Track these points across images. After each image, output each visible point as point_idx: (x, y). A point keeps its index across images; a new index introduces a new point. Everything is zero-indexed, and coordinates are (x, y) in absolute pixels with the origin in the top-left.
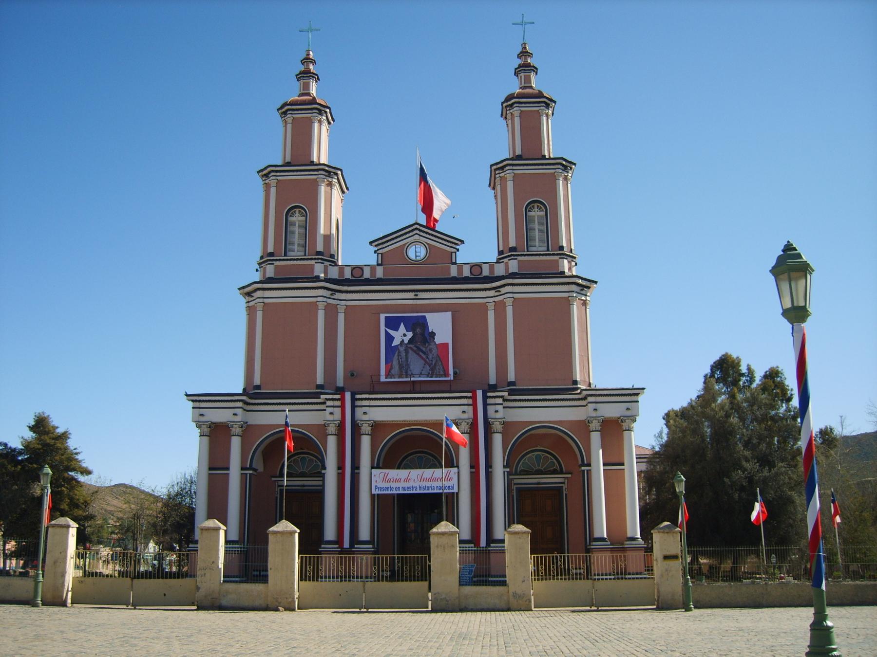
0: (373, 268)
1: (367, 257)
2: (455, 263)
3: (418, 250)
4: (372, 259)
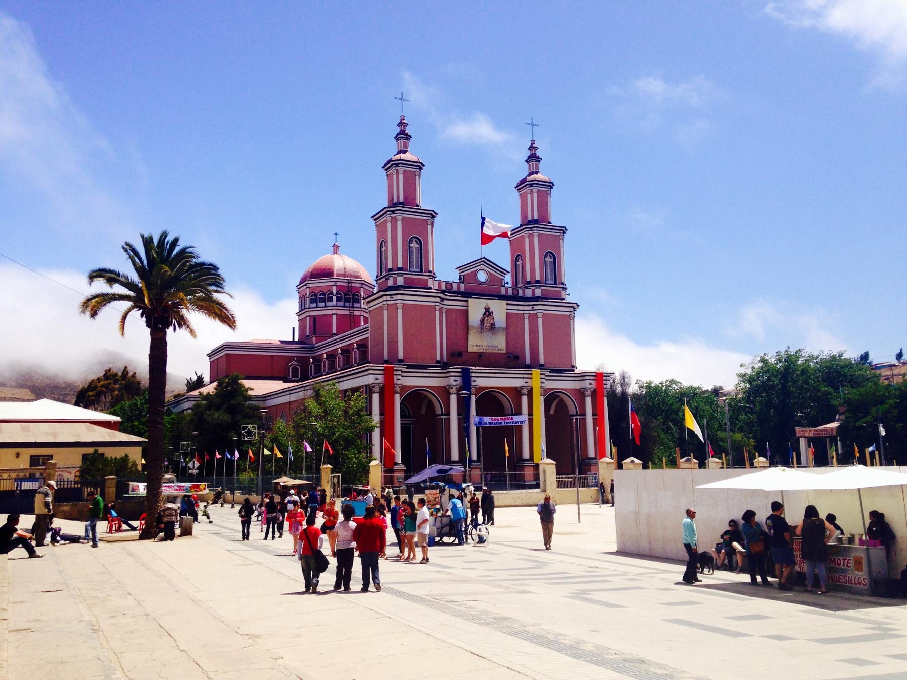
1: (454, 277)
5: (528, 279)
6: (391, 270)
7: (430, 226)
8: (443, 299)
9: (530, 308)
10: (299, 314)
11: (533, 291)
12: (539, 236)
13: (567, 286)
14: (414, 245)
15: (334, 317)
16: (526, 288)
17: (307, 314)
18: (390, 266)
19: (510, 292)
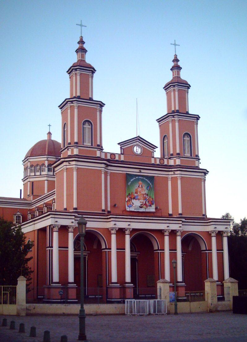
0: (119, 155)
1: (117, 150)
2: (153, 157)
3: (137, 149)
4: (119, 151)
5: (171, 152)
6: (70, 144)
7: (98, 113)
8: (107, 165)
10: (24, 180)
12: (179, 121)
13: (200, 158)
15: (46, 182)
16: (170, 158)
17: (28, 180)
18: (69, 141)
19: (158, 162)
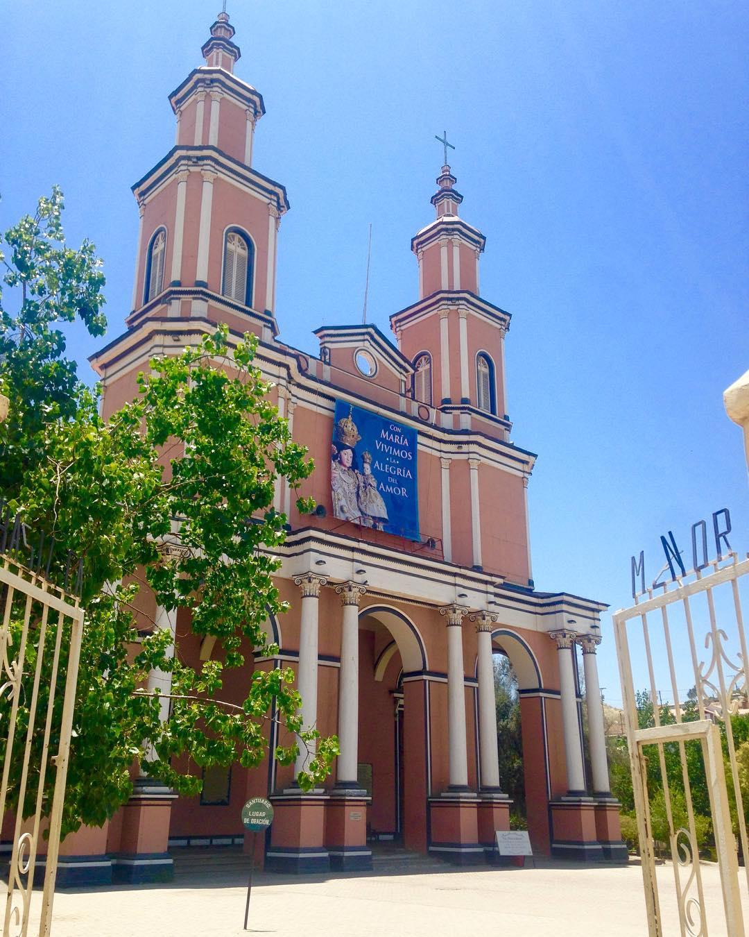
5: (446, 394)
7: (272, 221)
9: (453, 448)
11: (456, 420)
14: (237, 249)
16: (443, 410)
18: (176, 275)
